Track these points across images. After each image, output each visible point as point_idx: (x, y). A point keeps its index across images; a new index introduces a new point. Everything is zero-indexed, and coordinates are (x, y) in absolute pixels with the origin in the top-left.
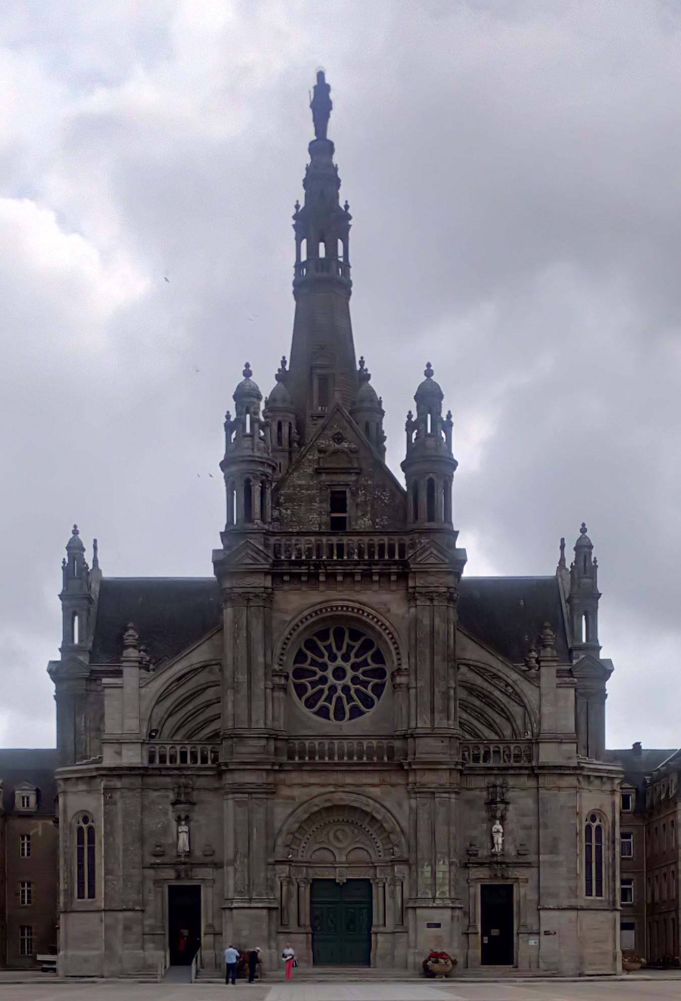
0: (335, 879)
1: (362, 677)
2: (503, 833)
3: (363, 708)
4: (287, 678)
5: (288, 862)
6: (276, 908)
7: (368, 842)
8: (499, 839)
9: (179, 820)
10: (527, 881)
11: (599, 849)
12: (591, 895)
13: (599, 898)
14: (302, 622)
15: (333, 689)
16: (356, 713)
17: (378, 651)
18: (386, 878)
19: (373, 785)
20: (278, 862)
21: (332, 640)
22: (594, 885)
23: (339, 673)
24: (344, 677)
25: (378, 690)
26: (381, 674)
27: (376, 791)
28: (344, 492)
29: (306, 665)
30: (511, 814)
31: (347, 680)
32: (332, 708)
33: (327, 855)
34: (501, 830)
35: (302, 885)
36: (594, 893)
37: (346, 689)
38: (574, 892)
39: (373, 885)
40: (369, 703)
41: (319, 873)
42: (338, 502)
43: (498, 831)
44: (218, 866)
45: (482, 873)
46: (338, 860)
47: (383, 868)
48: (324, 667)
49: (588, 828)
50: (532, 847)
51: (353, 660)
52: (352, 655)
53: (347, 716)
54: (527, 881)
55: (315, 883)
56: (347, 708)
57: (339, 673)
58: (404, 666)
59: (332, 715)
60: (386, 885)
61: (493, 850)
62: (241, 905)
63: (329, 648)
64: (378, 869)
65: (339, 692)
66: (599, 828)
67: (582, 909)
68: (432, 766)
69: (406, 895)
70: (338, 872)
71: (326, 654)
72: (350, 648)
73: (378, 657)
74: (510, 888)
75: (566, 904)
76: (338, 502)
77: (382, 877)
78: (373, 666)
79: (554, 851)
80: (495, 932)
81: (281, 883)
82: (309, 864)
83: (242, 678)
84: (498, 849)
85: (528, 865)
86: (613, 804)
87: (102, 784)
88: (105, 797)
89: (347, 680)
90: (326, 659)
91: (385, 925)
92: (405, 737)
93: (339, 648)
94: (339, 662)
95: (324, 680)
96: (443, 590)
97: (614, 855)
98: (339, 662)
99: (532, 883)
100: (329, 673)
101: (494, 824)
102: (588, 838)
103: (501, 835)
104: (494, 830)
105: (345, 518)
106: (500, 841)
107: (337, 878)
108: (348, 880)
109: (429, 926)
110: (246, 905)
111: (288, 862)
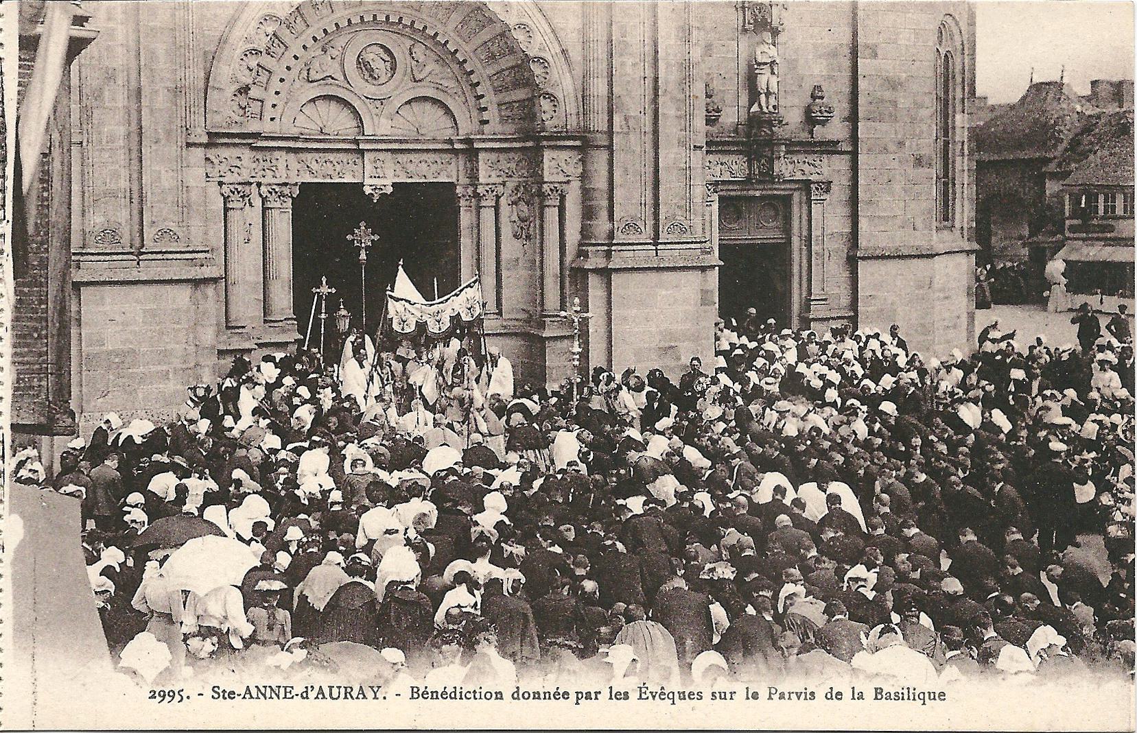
0: (362, 185)
5: (250, 140)
6: (215, 280)
7: (451, 84)
10: (827, 186)
18: (504, 184)
20: (214, 139)
33: (339, 123)
35: (274, 203)
39: (462, 203)
41: (314, 166)
46: (368, 130)
47: (494, 156)
50: (841, 108)
54: (827, 186)
60: (503, 201)
61: (755, 108)
64: (482, 156)
70: (368, 167)
77: (494, 179)
81: (226, 199)
82: (296, 146)
85: (829, 148)
99: (839, 192)
107: (368, 181)
111: (250, 140)
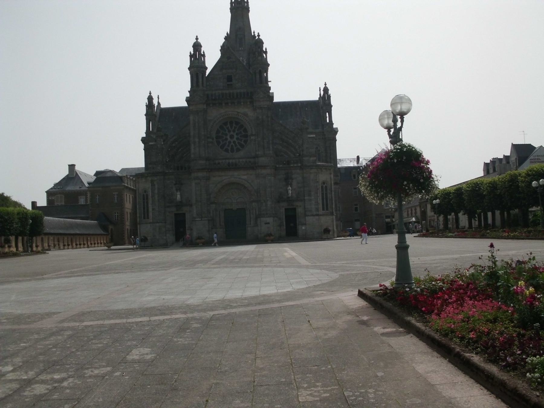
1: (239, 138)
2: (292, 190)
3: (241, 149)
4: (213, 139)
8: (290, 192)
9: (177, 190)
11: (326, 194)
12: (324, 210)
13: (327, 211)
14: (217, 120)
15: (230, 142)
16: (238, 150)
17: (245, 128)
19: (244, 175)
21: (229, 125)
22: (325, 206)
23: (232, 137)
24: (233, 138)
25: (246, 142)
26: (246, 136)
27: (245, 177)
28: (231, 76)
29: (220, 135)
30: (294, 183)
31: (235, 139)
32: (229, 148)
34: (291, 189)
36: (325, 210)
37: (234, 142)
38: (317, 210)
40: (242, 146)
42: (229, 79)
43: (290, 189)
44: (191, 206)
45: (285, 205)
48: (226, 135)
49: (322, 187)
51: (236, 132)
52: (236, 130)
53: (235, 151)
55: (226, 210)
56: (235, 148)
57: (232, 137)
58: (254, 133)
59: (230, 151)
62: (198, 219)
63: (228, 128)
65: (232, 144)
66: (326, 187)
67: (321, 215)
68: (264, 167)
69: (257, 213)
71: (227, 130)
72: (235, 128)
73: (245, 130)
74: (295, 209)
75: (315, 213)
76: (229, 79)
78: (243, 133)
79: (310, 195)
80: (292, 225)
83: (197, 140)
84: (290, 195)
86: (331, 178)
87: (150, 179)
88: (151, 183)
89: (235, 139)
90: (227, 132)
91: (251, 224)
92: (254, 158)
93: (231, 127)
94: (232, 133)
95: (226, 139)
96: (266, 106)
97: (332, 196)
98: (232, 133)
100: (228, 137)
101: (288, 186)
102: (322, 190)
103: (291, 190)
104: (288, 189)
105: (231, 85)
106: (291, 192)
108: (237, 209)
109: (266, 223)
110: (200, 219)
